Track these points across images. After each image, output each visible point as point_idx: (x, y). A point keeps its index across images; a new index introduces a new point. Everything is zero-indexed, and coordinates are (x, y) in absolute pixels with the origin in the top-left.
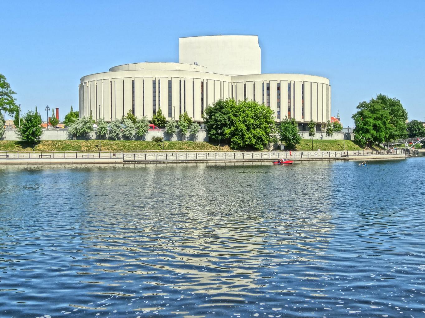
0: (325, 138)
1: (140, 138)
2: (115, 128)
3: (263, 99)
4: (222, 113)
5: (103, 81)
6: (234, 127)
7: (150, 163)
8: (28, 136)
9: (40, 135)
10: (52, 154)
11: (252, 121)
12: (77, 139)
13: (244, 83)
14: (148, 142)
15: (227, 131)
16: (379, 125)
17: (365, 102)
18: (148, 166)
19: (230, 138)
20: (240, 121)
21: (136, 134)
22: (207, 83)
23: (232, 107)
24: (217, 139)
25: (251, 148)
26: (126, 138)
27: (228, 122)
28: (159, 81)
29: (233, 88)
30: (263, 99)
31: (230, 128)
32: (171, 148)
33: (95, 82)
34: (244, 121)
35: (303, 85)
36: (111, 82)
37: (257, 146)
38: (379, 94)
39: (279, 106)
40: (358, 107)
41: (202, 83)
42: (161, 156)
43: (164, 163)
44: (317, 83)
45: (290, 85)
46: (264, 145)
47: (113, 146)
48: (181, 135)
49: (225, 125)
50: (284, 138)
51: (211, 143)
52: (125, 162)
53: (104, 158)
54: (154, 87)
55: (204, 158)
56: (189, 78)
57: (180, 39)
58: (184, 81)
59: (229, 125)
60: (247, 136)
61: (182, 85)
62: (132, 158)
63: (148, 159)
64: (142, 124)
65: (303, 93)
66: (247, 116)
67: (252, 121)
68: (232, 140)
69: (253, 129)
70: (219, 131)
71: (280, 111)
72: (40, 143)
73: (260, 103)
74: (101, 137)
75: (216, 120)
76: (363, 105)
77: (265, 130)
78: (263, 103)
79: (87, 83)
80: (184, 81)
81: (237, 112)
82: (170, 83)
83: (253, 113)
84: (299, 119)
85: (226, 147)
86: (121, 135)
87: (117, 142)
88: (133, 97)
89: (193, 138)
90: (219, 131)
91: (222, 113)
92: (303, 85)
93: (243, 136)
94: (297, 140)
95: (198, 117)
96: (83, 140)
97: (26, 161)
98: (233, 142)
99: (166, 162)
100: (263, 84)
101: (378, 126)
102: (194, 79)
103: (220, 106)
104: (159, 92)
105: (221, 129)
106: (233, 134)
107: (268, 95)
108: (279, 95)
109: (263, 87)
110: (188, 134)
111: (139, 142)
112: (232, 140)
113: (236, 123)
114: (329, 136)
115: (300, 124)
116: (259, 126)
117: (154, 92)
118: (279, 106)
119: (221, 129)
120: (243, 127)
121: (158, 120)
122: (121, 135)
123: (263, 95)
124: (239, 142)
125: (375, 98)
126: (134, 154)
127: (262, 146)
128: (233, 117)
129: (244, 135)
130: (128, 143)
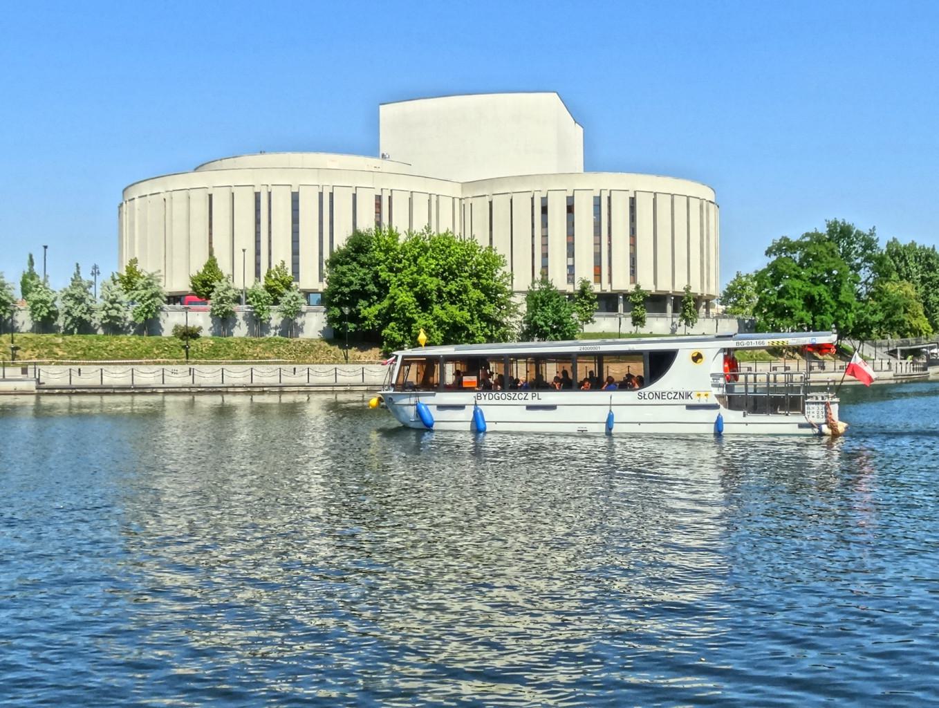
1: (149, 326)
5: (162, 196)
7: (114, 394)
13: (487, 199)
15: (370, 311)
16: (820, 295)
17: (786, 239)
18: (230, 400)
24: (350, 334)
26: (114, 327)
27: (372, 287)
29: (463, 208)
32: (214, 355)
35: (633, 201)
38: (831, 219)
40: (769, 252)
43: (152, 393)
47: (56, 350)
49: (365, 295)
55: (274, 380)
57: (381, 106)
58: (331, 195)
60: (422, 322)
63: (107, 380)
65: (633, 219)
66: (420, 271)
67: (432, 283)
68: (386, 332)
70: (346, 311)
71: (573, 266)
73: (483, 242)
74: (45, 324)
76: (784, 247)
82: (295, 198)
88: (211, 234)
89: (290, 327)
90: (346, 311)
91: (359, 263)
92: (633, 201)
95: (311, 278)
99: (161, 391)
101: (817, 298)
102: (391, 190)
103: (359, 246)
105: (352, 304)
106: (385, 318)
107: (545, 225)
116: (454, 298)
118: (571, 253)
120: (405, 298)
125: (823, 230)
126: (79, 370)
129: (413, 321)
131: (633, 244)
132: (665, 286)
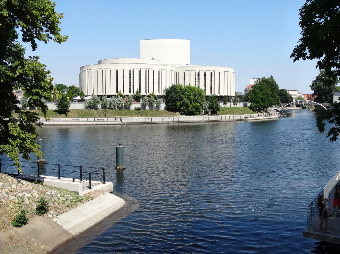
0: (233, 106)
1: (127, 107)
2: (113, 102)
3: (196, 82)
4: (175, 93)
5: (97, 70)
6: (182, 101)
8: (62, 107)
9: (69, 107)
10: (79, 119)
11: (193, 98)
12: (90, 109)
14: (132, 110)
15: (179, 104)
16: (264, 98)
19: (180, 108)
20: (186, 97)
21: (125, 105)
22: (162, 71)
23: (181, 89)
25: (192, 114)
26: (119, 108)
28: (133, 70)
29: (177, 75)
30: (196, 82)
31: (180, 102)
32: (146, 114)
33: (92, 70)
34: (188, 98)
35: (219, 73)
36: (103, 70)
37: (195, 113)
39: (205, 86)
41: (159, 71)
42: (143, 119)
45: (212, 73)
46: (199, 111)
47: (112, 113)
48: (151, 105)
49: (177, 100)
50: (210, 107)
51: (169, 111)
52: (123, 124)
53: (109, 121)
54: (130, 74)
56: (151, 68)
57: (141, 41)
58: (148, 71)
59: (179, 100)
60: (190, 107)
61: (147, 72)
62: (126, 121)
63: (135, 121)
64: (129, 99)
65: (219, 78)
68: (181, 109)
69: (193, 102)
70: (174, 104)
72: (69, 111)
74: (104, 107)
75: (172, 97)
77: (200, 103)
78: (196, 84)
79: (87, 70)
80: (148, 71)
81: (184, 92)
82: (140, 72)
83: (193, 93)
84: (217, 94)
85: (178, 113)
86: (116, 106)
87: (114, 110)
89: (158, 107)
91: (175, 93)
92: (219, 73)
93: (187, 107)
94: (218, 108)
96: (94, 110)
97: (65, 123)
98: (181, 110)
100: (196, 72)
101: (264, 98)
103: (173, 89)
104: (133, 77)
105: (175, 102)
106: (181, 105)
107: (199, 79)
108: (205, 79)
109: (196, 74)
110: (155, 105)
111: (127, 110)
112: (181, 109)
113: (183, 99)
114: (235, 105)
115: (217, 97)
116: (196, 101)
117: (130, 77)
118: (205, 86)
119: (175, 102)
120: (187, 101)
121: (137, 97)
122: (116, 106)
123: (196, 79)
124: (185, 110)
127: (198, 112)
128: (181, 95)
129: (189, 106)
130: (121, 111)
131: (219, 84)
132: (226, 94)
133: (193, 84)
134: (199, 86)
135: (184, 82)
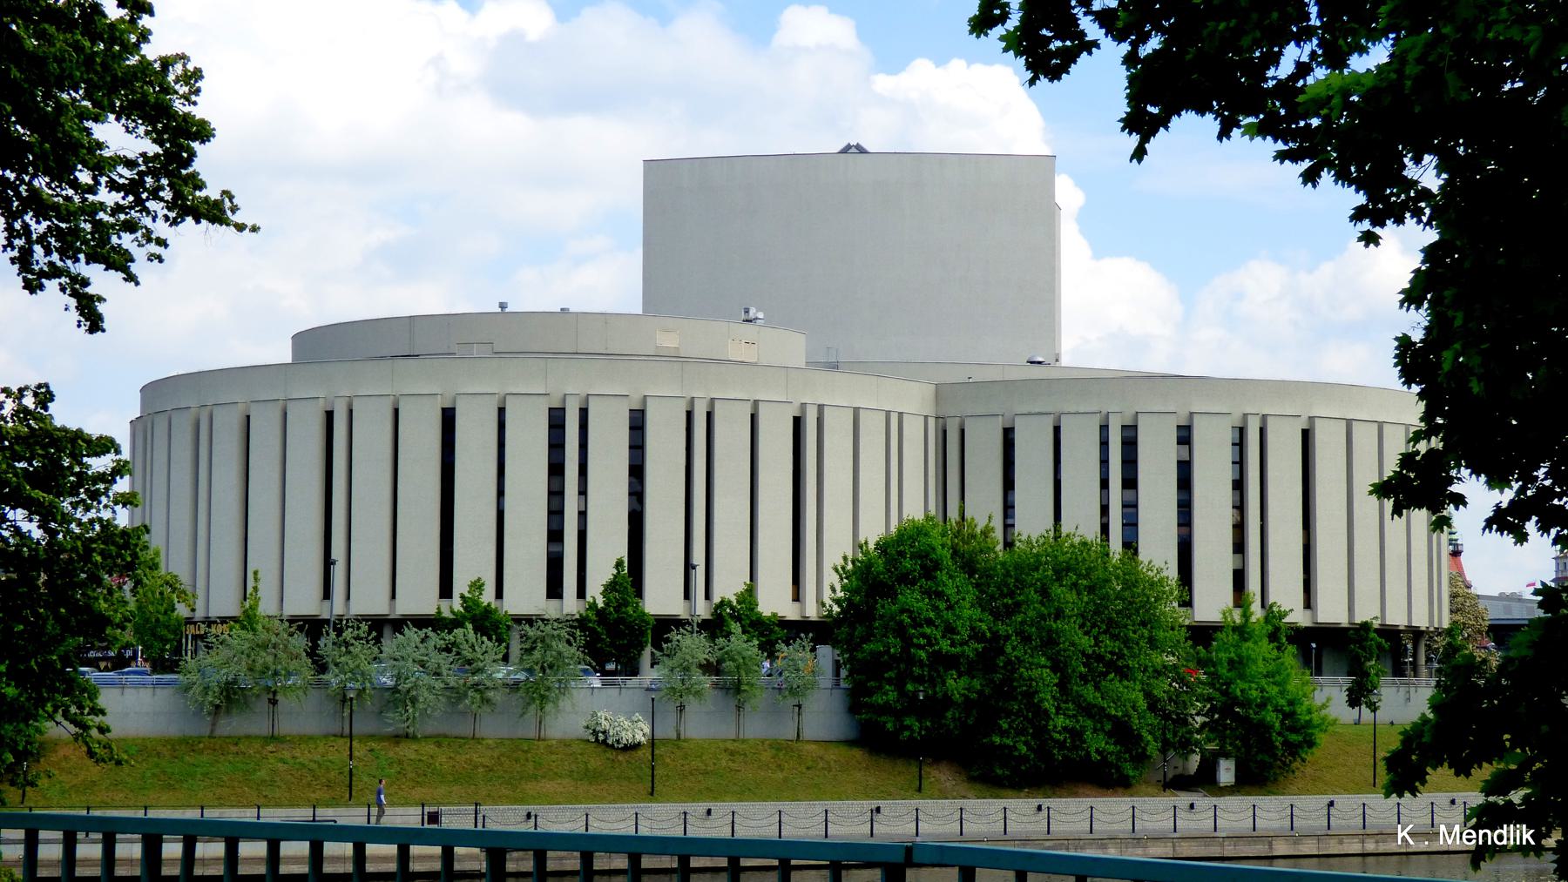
28: (584, 413)
29: (949, 446)
30: (1105, 510)
35: (1307, 436)
44: (1381, 425)
45: (1242, 431)
58: (710, 415)
61: (699, 428)
78: (1105, 529)
80: (710, 415)
92: (1307, 436)
100: (1104, 429)
109: (1104, 444)
117: (556, 469)
123: (1105, 484)
132: (1366, 612)
133: (1081, 521)
134: (1130, 545)
135: (1008, 508)
